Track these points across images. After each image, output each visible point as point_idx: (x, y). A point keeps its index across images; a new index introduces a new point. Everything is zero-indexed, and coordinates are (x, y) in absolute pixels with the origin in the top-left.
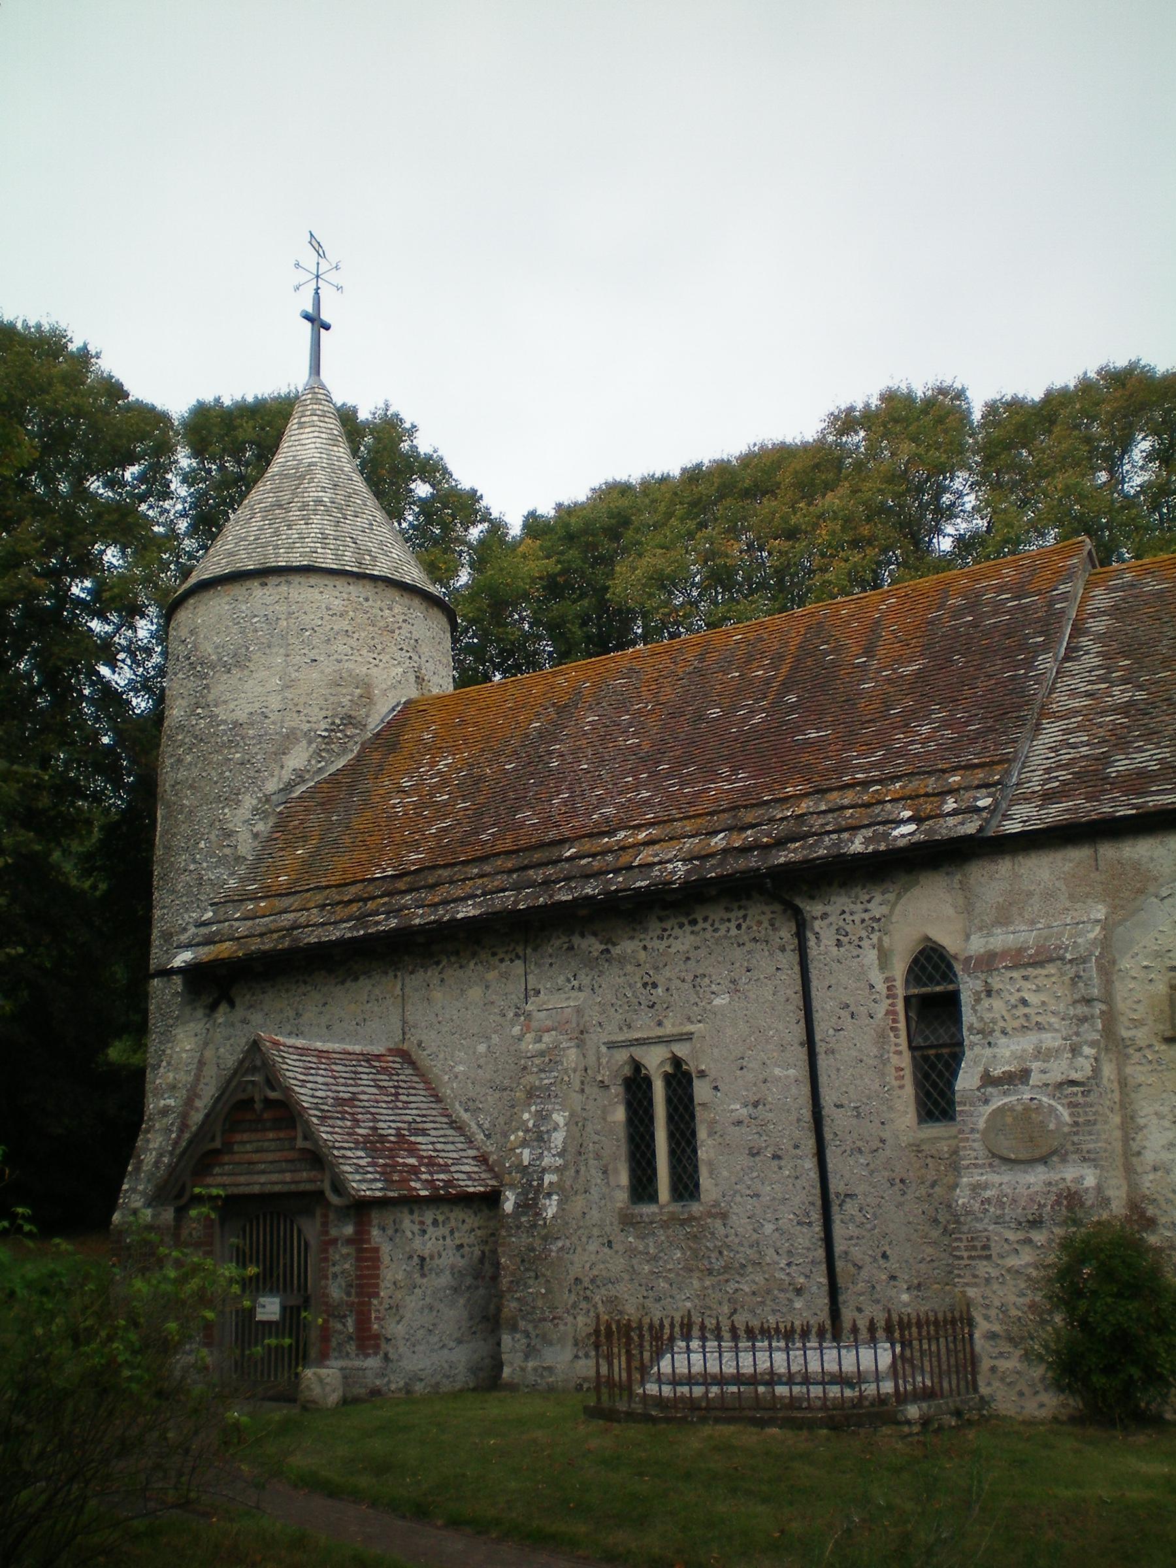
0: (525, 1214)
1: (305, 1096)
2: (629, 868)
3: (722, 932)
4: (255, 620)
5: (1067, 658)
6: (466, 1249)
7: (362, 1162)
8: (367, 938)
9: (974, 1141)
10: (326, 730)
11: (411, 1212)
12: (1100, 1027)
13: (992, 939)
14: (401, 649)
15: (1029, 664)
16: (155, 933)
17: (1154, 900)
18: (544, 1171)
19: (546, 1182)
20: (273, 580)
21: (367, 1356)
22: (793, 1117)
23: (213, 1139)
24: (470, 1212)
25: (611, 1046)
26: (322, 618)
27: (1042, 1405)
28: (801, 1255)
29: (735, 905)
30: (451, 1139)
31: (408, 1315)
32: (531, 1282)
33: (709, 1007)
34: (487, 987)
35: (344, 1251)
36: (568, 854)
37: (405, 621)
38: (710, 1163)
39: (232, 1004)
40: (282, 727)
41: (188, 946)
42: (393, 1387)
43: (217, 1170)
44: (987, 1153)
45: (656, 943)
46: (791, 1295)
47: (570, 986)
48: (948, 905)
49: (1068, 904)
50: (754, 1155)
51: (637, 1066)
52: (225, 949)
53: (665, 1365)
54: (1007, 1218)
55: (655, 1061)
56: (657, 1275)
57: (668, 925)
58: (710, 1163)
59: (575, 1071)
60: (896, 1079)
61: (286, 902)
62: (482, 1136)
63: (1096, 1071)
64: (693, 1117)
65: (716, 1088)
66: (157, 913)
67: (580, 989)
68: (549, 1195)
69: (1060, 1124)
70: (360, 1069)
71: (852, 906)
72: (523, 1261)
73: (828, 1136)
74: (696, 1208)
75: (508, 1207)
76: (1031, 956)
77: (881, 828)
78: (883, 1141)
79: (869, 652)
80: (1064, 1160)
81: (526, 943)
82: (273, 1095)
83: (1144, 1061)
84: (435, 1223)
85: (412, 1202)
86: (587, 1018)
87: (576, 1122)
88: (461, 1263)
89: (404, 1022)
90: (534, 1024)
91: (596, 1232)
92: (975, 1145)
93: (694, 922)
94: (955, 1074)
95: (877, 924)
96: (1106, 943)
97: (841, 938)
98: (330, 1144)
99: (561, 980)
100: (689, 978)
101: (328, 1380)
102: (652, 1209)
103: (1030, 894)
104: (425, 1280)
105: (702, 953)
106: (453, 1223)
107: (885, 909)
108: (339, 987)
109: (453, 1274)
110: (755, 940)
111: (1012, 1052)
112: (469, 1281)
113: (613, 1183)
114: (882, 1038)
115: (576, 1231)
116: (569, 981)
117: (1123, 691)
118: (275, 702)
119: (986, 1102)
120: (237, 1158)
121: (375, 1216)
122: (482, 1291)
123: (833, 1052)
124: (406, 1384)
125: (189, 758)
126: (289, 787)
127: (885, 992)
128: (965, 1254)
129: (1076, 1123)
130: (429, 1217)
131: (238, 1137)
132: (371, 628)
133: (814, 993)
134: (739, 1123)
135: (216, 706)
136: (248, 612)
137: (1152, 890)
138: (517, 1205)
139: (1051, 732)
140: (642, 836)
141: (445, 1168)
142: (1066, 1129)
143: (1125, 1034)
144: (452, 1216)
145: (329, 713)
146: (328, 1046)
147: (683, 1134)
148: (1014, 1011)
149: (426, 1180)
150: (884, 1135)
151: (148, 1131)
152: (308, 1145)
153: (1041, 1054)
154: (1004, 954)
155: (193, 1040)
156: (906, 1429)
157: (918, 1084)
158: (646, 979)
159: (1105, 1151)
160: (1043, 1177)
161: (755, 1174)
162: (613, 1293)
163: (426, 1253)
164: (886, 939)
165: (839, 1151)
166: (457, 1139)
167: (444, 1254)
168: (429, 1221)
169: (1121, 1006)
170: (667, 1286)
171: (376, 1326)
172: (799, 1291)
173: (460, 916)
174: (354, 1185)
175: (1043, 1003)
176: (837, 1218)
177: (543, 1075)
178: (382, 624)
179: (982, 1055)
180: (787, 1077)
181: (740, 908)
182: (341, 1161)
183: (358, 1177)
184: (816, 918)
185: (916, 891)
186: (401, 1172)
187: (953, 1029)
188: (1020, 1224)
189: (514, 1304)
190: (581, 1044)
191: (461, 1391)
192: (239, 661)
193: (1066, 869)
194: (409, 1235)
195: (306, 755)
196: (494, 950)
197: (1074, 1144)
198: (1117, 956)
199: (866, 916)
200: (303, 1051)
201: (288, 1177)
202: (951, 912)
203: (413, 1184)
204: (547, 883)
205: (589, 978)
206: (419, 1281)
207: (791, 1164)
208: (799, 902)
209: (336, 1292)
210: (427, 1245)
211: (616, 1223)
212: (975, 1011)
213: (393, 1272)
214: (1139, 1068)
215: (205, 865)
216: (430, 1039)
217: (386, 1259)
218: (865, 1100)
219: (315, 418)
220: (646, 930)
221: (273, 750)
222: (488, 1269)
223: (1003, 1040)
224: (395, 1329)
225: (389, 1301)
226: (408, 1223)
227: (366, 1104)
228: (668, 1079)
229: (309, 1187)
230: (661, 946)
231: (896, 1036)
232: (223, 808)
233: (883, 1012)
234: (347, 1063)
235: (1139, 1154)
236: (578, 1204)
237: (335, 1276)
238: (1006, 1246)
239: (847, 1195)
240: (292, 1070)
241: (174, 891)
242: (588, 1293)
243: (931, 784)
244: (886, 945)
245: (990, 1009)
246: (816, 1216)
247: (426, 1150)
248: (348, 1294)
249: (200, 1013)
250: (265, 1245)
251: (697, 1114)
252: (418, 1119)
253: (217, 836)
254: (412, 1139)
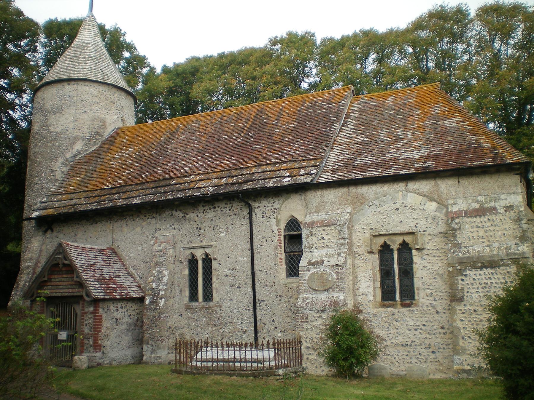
0: (152, 305)
1: (77, 263)
2: (194, 188)
3: (224, 212)
4: (65, 96)
5: (343, 125)
6: (132, 316)
7: (97, 286)
8: (102, 209)
9: (304, 283)
10: (89, 136)
11: (113, 303)
12: (347, 247)
13: (313, 217)
14: (117, 110)
15: (331, 126)
16: (26, 205)
17: (367, 206)
18: (160, 290)
19: (160, 294)
20: (72, 83)
21: (97, 352)
22: (245, 274)
23: (44, 277)
24: (134, 304)
25: (185, 249)
26: (89, 97)
27: (323, 371)
28: (246, 320)
29: (229, 202)
30: (128, 279)
31: (111, 338)
32: (154, 328)
33: (218, 236)
34: (142, 227)
35: (90, 316)
36: (172, 183)
37: (118, 100)
38: (217, 289)
39: (52, 231)
40: (73, 135)
41: (37, 210)
42: (105, 362)
43: (46, 288)
44: (308, 287)
45: (201, 214)
46: (242, 333)
47: (171, 228)
48: (300, 205)
49: (339, 207)
50: (231, 287)
51: (193, 256)
52: (50, 212)
53: (199, 356)
54: (314, 309)
55: (199, 254)
56: (197, 326)
58: (217, 289)
59: (172, 257)
60: (280, 262)
61: (72, 196)
62: (139, 278)
63: (345, 261)
64: (211, 273)
65: (220, 264)
66: (26, 198)
67: (175, 229)
68: (161, 298)
69: (333, 279)
70: (97, 254)
71: (268, 204)
72: (151, 320)
73: (256, 281)
74: (211, 304)
75: (147, 302)
76: (326, 223)
77: (279, 179)
78: (274, 283)
79: (278, 119)
80: (333, 291)
81: (157, 213)
82: (66, 262)
83: (361, 259)
84: (122, 307)
85: (114, 300)
86: (176, 239)
87: (172, 274)
88: (130, 321)
89: (113, 239)
90: (158, 241)
91: (177, 311)
92: (305, 285)
93: (215, 208)
94: (299, 261)
95: (276, 211)
96: (351, 220)
97: (264, 215)
98: (86, 279)
99: (168, 226)
100: (212, 226)
101: (83, 360)
102: (197, 304)
103: (327, 203)
104: (118, 327)
105: (217, 218)
106: (128, 308)
107: (279, 206)
108: (90, 226)
109: (127, 325)
111: (318, 255)
112: (133, 327)
113: (183, 295)
114: (276, 248)
115: (170, 311)
116: (171, 226)
117: (361, 137)
118: (71, 126)
119: (309, 271)
120: (53, 284)
121: (101, 305)
122: (137, 330)
123: (259, 253)
124: (110, 361)
125: (39, 144)
126: (75, 156)
127: (277, 233)
128: (300, 321)
129: (338, 278)
130: (119, 305)
131: (53, 277)
132: (106, 102)
133: (254, 233)
134: (227, 275)
135: (50, 126)
136: (63, 94)
137: (366, 203)
138: (150, 302)
139: (337, 150)
140: (198, 178)
141: (126, 289)
142: (334, 280)
143: (355, 250)
144: (128, 305)
145: (90, 131)
146: (86, 246)
147: (208, 279)
148: (319, 241)
149: (119, 293)
150: (275, 281)
151: (21, 274)
152: (78, 280)
153: (327, 255)
154: (317, 222)
155: (38, 243)
156: (278, 377)
157: (287, 264)
158: (197, 227)
159: (347, 288)
160: (326, 296)
161: (231, 293)
162: (182, 332)
163: (118, 317)
164: (279, 216)
165: (260, 285)
166: (130, 279)
167: (124, 318)
168: (119, 307)
169: (354, 241)
170: (200, 330)
171: (100, 342)
172: (244, 332)
173: (134, 203)
174: (94, 294)
175: (329, 239)
176: (258, 308)
177: (161, 258)
178: (110, 100)
179: (308, 255)
180: (244, 261)
181: (230, 203)
182: (89, 285)
183: (95, 291)
184: (256, 208)
185: (289, 200)
186: (110, 290)
187: (299, 246)
188: (318, 311)
189: (148, 335)
190: (174, 248)
191: (128, 364)
192: (59, 111)
193: (339, 195)
194: (112, 311)
195: (81, 145)
196: (146, 215)
197: (337, 285)
198: (354, 224)
199: (273, 208)
200: (77, 248)
201: (70, 290)
202: (301, 207)
203: (114, 294)
204: (165, 192)
205: (178, 225)
206: (115, 327)
207: (244, 290)
208: (250, 202)
209: (86, 330)
210: (118, 315)
211: (184, 308)
212: (307, 241)
213: (106, 323)
214: (359, 261)
215: (44, 182)
216: (122, 244)
217: (104, 319)
218: (269, 269)
219: (90, 27)
220: (198, 210)
221: (70, 142)
222: (139, 324)
223: (315, 251)
224: (107, 343)
225: (105, 333)
226: (112, 307)
227: (99, 266)
228: (204, 260)
229: (78, 294)
231: (281, 248)
232: (51, 162)
233: (277, 240)
234: (93, 252)
235: (358, 289)
236: (171, 301)
237: (86, 325)
238: (313, 318)
239: (261, 300)
240: (73, 254)
241: (33, 191)
242: (173, 331)
243: (296, 165)
244: (278, 218)
245: (312, 240)
246: (251, 307)
247: (119, 282)
248: (91, 331)
249: (41, 233)
250: (62, 313)
251: (213, 272)
252: (117, 272)
253: (49, 172)
254: (115, 278)
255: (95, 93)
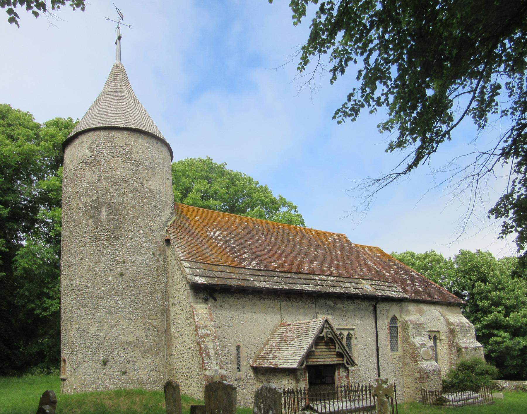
45: (346, 306)
57: (349, 302)
95: (387, 311)
99: (324, 311)
100: (353, 315)
110: (366, 310)
220: (344, 303)
230: (347, 307)
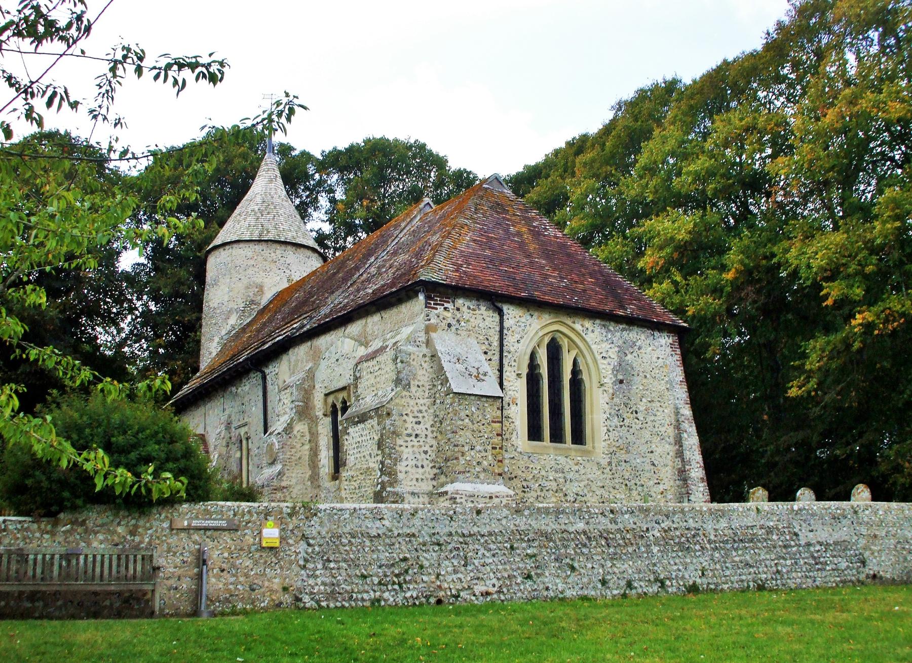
20: (227, 247)
126: (230, 332)
255: (250, 254)
